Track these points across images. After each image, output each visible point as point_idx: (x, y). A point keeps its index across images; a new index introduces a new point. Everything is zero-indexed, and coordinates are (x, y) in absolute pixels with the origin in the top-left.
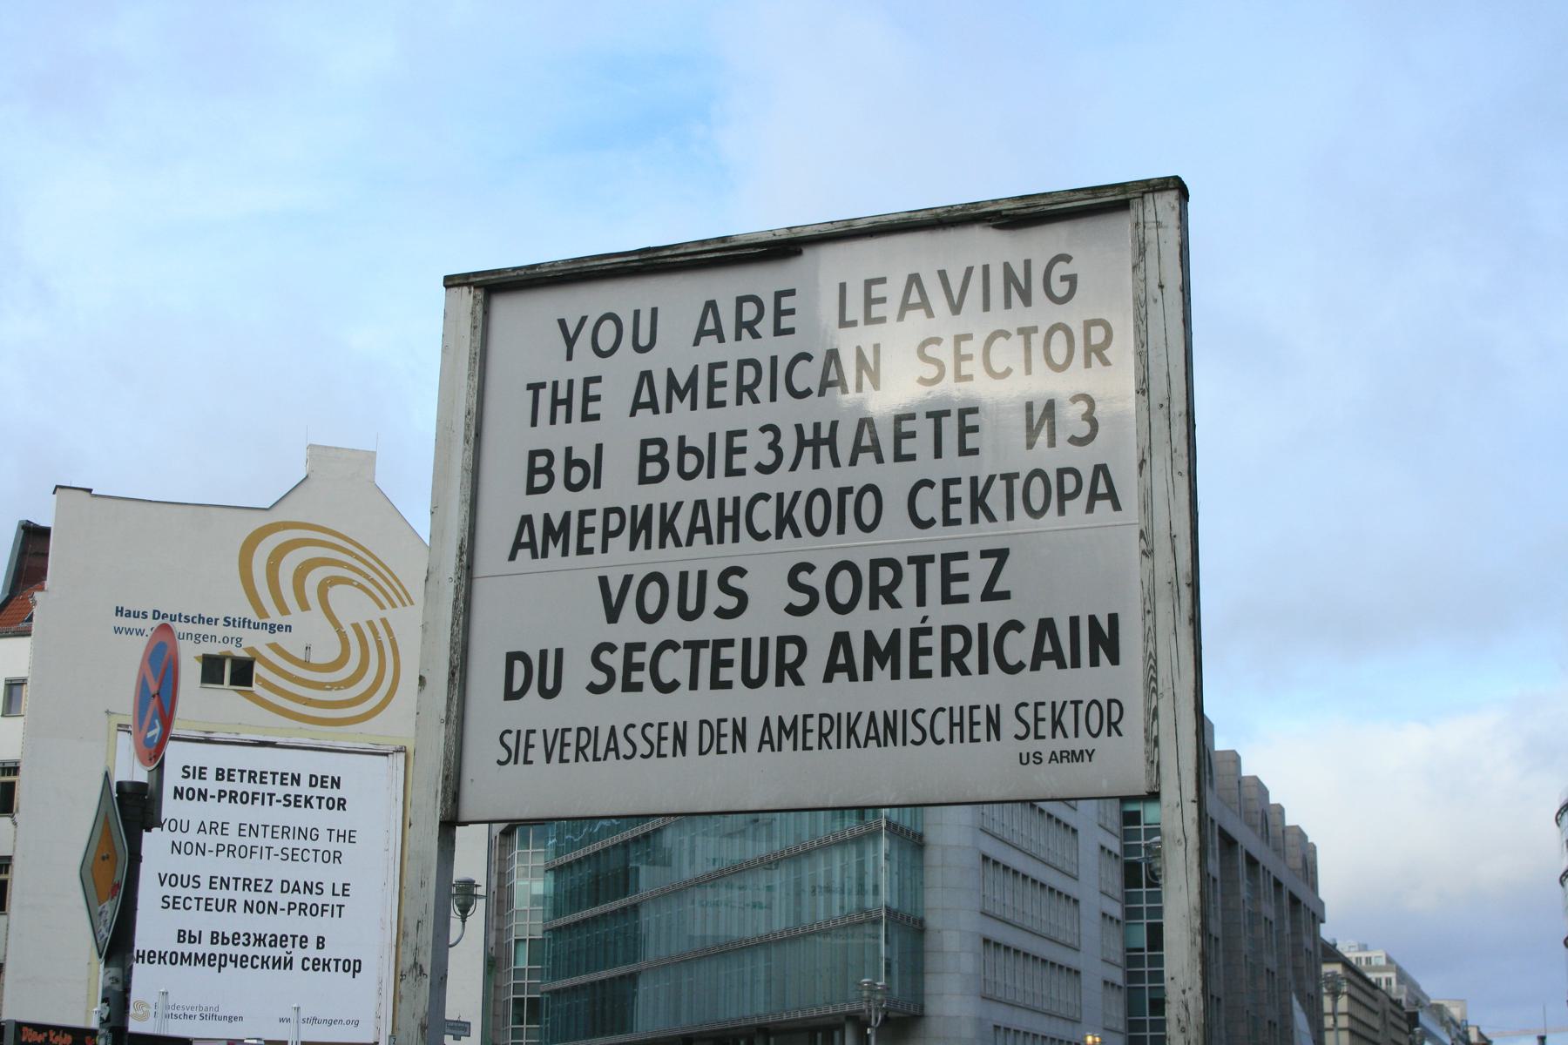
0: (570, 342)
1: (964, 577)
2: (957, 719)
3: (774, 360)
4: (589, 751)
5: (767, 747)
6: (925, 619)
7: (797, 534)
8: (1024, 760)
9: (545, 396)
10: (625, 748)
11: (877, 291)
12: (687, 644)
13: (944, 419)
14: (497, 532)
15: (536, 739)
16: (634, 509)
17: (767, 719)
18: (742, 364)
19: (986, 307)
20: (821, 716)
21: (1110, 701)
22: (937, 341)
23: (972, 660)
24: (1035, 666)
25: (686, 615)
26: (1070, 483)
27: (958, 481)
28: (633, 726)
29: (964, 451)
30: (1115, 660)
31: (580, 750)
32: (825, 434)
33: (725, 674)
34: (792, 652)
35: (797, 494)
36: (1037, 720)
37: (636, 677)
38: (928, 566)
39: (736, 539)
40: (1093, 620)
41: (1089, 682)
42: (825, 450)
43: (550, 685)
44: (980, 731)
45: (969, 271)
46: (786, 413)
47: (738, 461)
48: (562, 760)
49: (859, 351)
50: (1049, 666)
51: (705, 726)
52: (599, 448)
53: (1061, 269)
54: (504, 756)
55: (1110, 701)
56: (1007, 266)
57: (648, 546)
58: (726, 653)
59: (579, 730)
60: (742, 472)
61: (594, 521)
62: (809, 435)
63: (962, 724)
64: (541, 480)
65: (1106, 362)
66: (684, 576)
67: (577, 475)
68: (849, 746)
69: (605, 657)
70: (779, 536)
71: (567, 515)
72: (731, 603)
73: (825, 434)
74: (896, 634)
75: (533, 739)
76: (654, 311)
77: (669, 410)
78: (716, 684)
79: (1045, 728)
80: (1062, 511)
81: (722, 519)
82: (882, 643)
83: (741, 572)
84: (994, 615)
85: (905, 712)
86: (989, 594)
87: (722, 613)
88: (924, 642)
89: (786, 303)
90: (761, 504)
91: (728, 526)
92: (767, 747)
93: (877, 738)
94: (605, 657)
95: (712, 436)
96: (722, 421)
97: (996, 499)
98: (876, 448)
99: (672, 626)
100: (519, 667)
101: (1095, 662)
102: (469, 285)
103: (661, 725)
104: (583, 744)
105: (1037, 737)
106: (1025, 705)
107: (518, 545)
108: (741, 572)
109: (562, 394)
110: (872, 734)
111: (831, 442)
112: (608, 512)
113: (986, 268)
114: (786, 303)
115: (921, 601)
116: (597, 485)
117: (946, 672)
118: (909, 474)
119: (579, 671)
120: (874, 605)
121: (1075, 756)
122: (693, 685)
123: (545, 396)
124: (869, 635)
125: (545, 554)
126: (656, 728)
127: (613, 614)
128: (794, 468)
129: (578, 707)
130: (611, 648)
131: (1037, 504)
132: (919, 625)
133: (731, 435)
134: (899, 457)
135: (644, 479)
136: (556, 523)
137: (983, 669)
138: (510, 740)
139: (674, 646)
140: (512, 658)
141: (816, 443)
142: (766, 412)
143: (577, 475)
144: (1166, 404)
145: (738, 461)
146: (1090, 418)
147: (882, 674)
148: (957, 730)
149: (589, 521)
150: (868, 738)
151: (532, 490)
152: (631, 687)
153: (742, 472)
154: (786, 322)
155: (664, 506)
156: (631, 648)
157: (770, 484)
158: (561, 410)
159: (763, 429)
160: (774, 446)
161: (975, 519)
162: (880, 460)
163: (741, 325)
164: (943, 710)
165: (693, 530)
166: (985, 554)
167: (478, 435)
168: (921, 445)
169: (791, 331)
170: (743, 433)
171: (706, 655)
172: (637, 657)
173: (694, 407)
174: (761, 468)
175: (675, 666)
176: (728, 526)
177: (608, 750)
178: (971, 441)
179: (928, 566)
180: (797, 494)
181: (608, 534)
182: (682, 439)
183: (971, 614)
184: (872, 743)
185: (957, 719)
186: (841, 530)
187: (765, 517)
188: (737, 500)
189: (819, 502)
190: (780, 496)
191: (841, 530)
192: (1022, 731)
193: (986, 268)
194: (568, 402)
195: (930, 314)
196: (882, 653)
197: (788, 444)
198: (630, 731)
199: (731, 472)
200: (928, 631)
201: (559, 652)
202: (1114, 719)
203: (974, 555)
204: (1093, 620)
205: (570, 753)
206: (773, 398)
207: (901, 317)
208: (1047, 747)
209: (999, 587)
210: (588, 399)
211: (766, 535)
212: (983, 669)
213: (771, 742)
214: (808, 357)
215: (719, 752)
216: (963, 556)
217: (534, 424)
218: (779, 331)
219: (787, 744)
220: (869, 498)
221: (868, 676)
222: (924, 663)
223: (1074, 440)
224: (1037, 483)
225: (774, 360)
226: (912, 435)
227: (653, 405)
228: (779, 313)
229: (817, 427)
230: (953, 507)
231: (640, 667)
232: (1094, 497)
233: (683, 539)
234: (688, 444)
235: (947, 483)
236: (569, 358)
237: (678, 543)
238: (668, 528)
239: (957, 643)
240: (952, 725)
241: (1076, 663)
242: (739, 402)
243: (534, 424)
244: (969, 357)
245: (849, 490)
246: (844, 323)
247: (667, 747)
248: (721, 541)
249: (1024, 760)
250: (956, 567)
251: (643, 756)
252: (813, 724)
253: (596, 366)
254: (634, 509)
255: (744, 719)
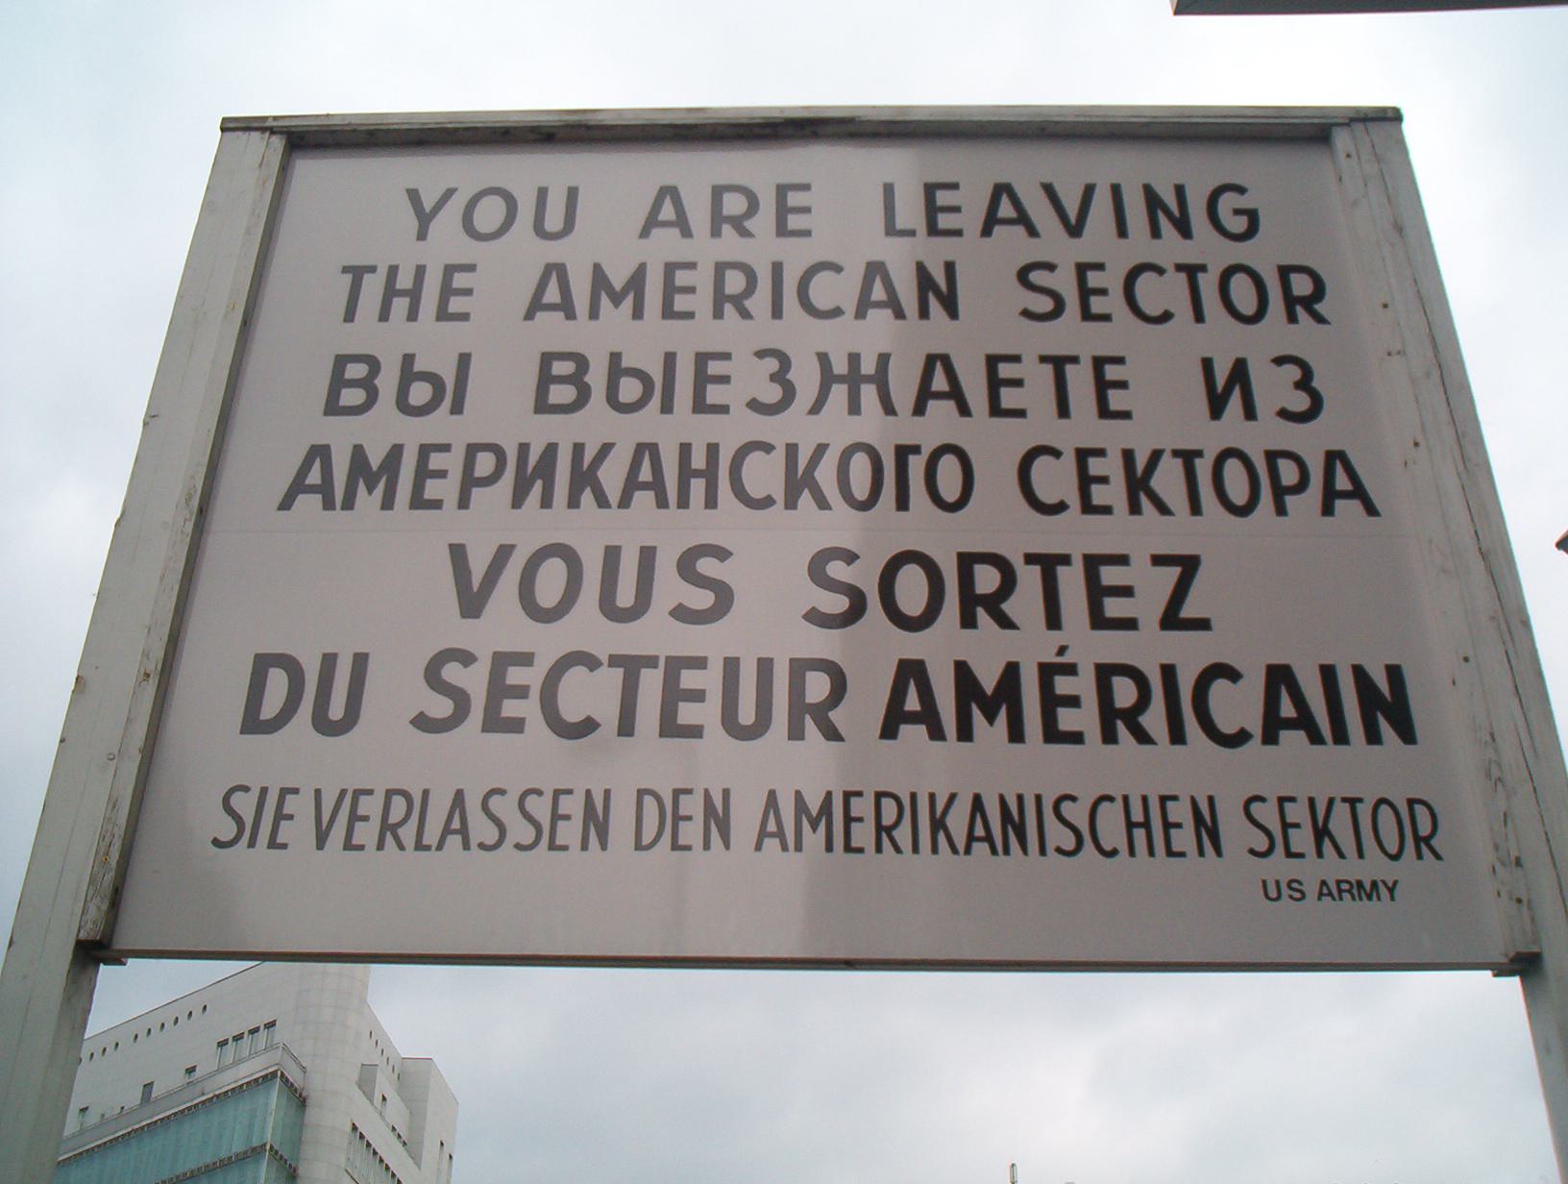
0: (425, 221)
1: (1126, 591)
2: (1137, 816)
3: (777, 269)
4: (408, 833)
5: (772, 844)
6: (1062, 651)
7: (823, 504)
8: (1271, 892)
9: (373, 288)
10: (482, 830)
11: (943, 198)
12: (615, 661)
13: (1069, 368)
14: (265, 458)
15: (300, 806)
16: (524, 449)
17: (772, 794)
18: (721, 268)
19: (1122, 232)
20: (879, 796)
21: (1411, 802)
22: (1050, 267)
23: (1155, 719)
24: (1270, 738)
25: (610, 610)
26: (1289, 474)
27: (1100, 453)
28: (502, 792)
29: (1104, 412)
30: (1407, 734)
31: (388, 828)
32: (868, 367)
33: (687, 713)
34: (818, 687)
35: (821, 449)
36: (1286, 826)
37: (510, 708)
38: (1062, 571)
39: (711, 502)
40: (1359, 672)
41: (1364, 768)
42: (869, 393)
43: (337, 711)
44: (1184, 838)
45: (1089, 191)
46: (804, 339)
47: (714, 394)
48: (349, 846)
49: (921, 268)
50: (1293, 739)
51: (649, 800)
52: (464, 360)
53: (1227, 203)
54: (228, 831)
55: (1411, 802)
56: (1148, 190)
57: (546, 502)
58: (689, 679)
59: (389, 794)
60: (724, 409)
61: (452, 462)
62: (840, 367)
63: (1148, 825)
64: (352, 397)
65: (1320, 319)
66: (612, 555)
67: (420, 393)
68: (935, 850)
69: (452, 672)
70: (791, 504)
71: (396, 451)
72: (703, 599)
73: (868, 367)
74: (1012, 671)
75: (291, 804)
76: (573, 193)
77: (594, 314)
78: (670, 727)
79: (1302, 839)
80: (1281, 510)
81: (686, 473)
82: (989, 681)
83: (721, 554)
84: (1190, 654)
85: (1038, 798)
86: (1172, 620)
87: (682, 613)
88: (1063, 685)
89: (794, 199)
90: (755, 459)
91: (698, 486)
92: (772, 844)
93: (988, 838)
94: (452, 672)
95: (670, 359)
96: (687, 340)
97: (1168, 480)
98: (956, 394)
99: (586, 628)
100: (277, 682)
101: (1373, 737)
102: (263, 130)
103: (557, 793)
104: (394, 818)
105: (1289, 854)
106: (1261, 799)
107: (299, 486)
108: (721, 554)
109: (405, 281)
110: (979, 831)
111: (881, 379)
112: (472, 450)
113: (1116, 191)
114: (794, 199)
115: (1053, 621)
116: (457, 408)
117: (1109, 737)
118: (1013, 439)
119: (396, 691)
120: (968, 621)
121: (1366, 891)
122: (626, 726)
123: (373, 288)
124: (962, 670)
125: (349, 504)
126: (548, 797)
127: (472, 603)
128: (816, 409)
129: (383, 752)
130: (466, 658)
131: (1238, 493)
132: (1051, 658)
133: (702, 359)
134: (996, 410)
135: (542, 406)
136: (375, 460)
137: (1177, 736)
138: (245, 805)
139: (591, 662)
140: (263, 664)
141: (854, 379)
142: (763, 330)
143: (420, 393)
144: (1436, 374)
145: (714, 394)
146: (1305, 383)
147: (990, 733)
148: (1139, 834)
149: (436, 461)
150: (971, 838)
151: (333, 408)
152: (494, 722)
153: (724, 409)
154: (794, 222)
155: (578, 449)
156: (502, 661)
157: (776, 430)
158: (401, 305)
159: (761, 354)
160: (780, 377)
161: (1135, 509)
162: (964, 410)
163: (718, 221)
164: (1110, 799)
165: (631, 485)
166: (1159, 560)
167: (247, 324)
168: (1035, 391)
169: (807, 233)
170: (726, 356)
171: (651, 682)
172: (515, 676)
173: (638, 313)
174: (754, 405)
175: (590, 695)
176: (698, 486)
177: (447, 831)
178: (1116, 400)
179: (1062, 571)
180: (821, 449)
181: (470, 482)
182: (615, 358)
183: (1148, 648)
184: (981, 849)
185: (1137, 816)
186: (902, 503)
187: (764, 475)
188: (713, 450)
189: (860, 465)
190: (792, 450)
191: (902, 503)
192: (1262, 844)
193: (1116, 191)
194: (415, 295)
195: (1033, 232)
196: (989, 700)
197: (805, 378)
198: (495, 802)
199: (700, 406)
200: (1070, 670)
201: (361, 661)
202: (1424, 829)
203: (1140, 560)
204: (1359, 672)
205: (367, 833)
206: (777, 312)
207: (987, 231)
208: (1312, 871)
209: (1188, 611)
210: (447, 291)
211: (767, 502)
212: (1177, 736)
213: (780, 834)
214: (837, 268)
215: (675, 846)
216: (1122, 560)
217: (350, 316)
218: (782, 230)
219: (814, 839)
220: (949, 467)
221: (965, 733)
222: (1067, 719)
223: (1284, 414)
224: (1233, 469)
225: (777, 269)
226: (1017, 383)
227: (567, 308)
228: (783, 211)
229: (854, 359)
230: (1095, 488)
231: (522, 692)
232: (1330, 498)
233: (613, 494)
234: (625, 363)
235: (1083, 455)
236: (422, 235)
237: (602, 502)
238: (584, 478)
239: (1125, 693)
240: (1130, 825)
241: (1341, 737)
242: (718, 314)
243: (350, 316)
244: (1103, 292)
245: (916, 450)
246: (891, 230)
247: (569, 832)
248: (683, 502)
249: (1271, 892)
250: (1110, 576)
251: (518, 846)
252: (862, 807)
253: (466, 250)
254: (524, 449)
255: (726, 793)
